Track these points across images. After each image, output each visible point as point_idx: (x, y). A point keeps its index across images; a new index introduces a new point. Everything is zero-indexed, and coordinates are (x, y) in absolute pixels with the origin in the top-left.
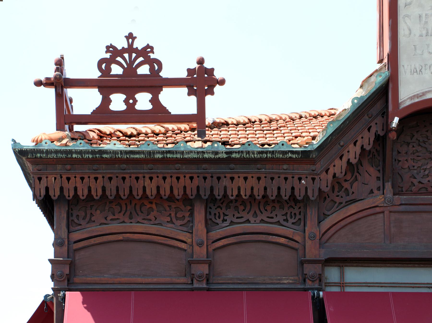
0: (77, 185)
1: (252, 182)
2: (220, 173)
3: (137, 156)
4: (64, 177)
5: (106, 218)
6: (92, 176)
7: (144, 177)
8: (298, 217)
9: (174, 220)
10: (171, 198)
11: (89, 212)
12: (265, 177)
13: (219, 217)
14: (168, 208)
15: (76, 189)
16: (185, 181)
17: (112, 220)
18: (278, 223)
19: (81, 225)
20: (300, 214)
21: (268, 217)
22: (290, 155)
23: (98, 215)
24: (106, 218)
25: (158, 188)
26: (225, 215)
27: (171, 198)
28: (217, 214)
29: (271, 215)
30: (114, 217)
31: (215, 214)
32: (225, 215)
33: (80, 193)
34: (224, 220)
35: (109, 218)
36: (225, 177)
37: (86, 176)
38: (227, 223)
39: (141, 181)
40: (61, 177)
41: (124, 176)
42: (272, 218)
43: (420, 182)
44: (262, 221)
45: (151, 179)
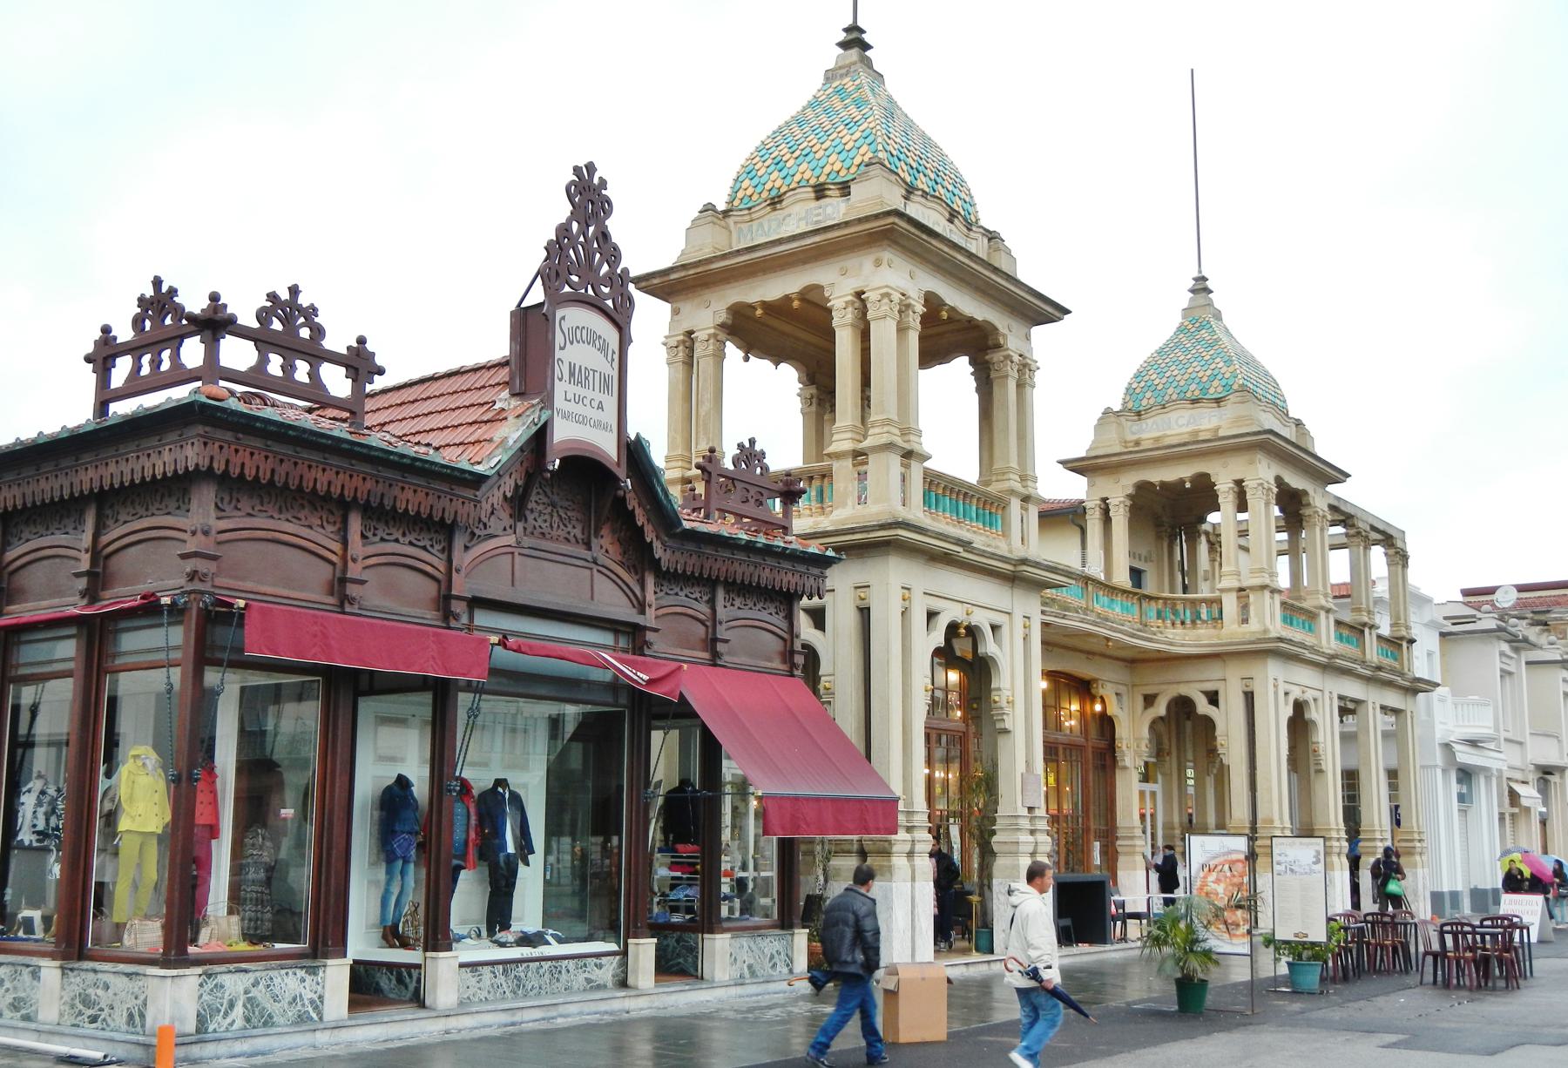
1: (421, 495)
2: (284, 454)
3: (324, 441)
5: (253, 509)
14: (320, 509)
15: (243, 465)
16: (357, 481)
17: (260, 511)
18: (424, 548)
19: (224, 511)
22: (467, 475)
23: (245, 505)
24: (253, 509)
25: (329, 483)
32: (376, 529)
33: (247, 472)
34: (375, 535)
35: (256, 509)
38: (377, 539)
39: (313, 471)
44: (411, 543)
45: (324, 470)
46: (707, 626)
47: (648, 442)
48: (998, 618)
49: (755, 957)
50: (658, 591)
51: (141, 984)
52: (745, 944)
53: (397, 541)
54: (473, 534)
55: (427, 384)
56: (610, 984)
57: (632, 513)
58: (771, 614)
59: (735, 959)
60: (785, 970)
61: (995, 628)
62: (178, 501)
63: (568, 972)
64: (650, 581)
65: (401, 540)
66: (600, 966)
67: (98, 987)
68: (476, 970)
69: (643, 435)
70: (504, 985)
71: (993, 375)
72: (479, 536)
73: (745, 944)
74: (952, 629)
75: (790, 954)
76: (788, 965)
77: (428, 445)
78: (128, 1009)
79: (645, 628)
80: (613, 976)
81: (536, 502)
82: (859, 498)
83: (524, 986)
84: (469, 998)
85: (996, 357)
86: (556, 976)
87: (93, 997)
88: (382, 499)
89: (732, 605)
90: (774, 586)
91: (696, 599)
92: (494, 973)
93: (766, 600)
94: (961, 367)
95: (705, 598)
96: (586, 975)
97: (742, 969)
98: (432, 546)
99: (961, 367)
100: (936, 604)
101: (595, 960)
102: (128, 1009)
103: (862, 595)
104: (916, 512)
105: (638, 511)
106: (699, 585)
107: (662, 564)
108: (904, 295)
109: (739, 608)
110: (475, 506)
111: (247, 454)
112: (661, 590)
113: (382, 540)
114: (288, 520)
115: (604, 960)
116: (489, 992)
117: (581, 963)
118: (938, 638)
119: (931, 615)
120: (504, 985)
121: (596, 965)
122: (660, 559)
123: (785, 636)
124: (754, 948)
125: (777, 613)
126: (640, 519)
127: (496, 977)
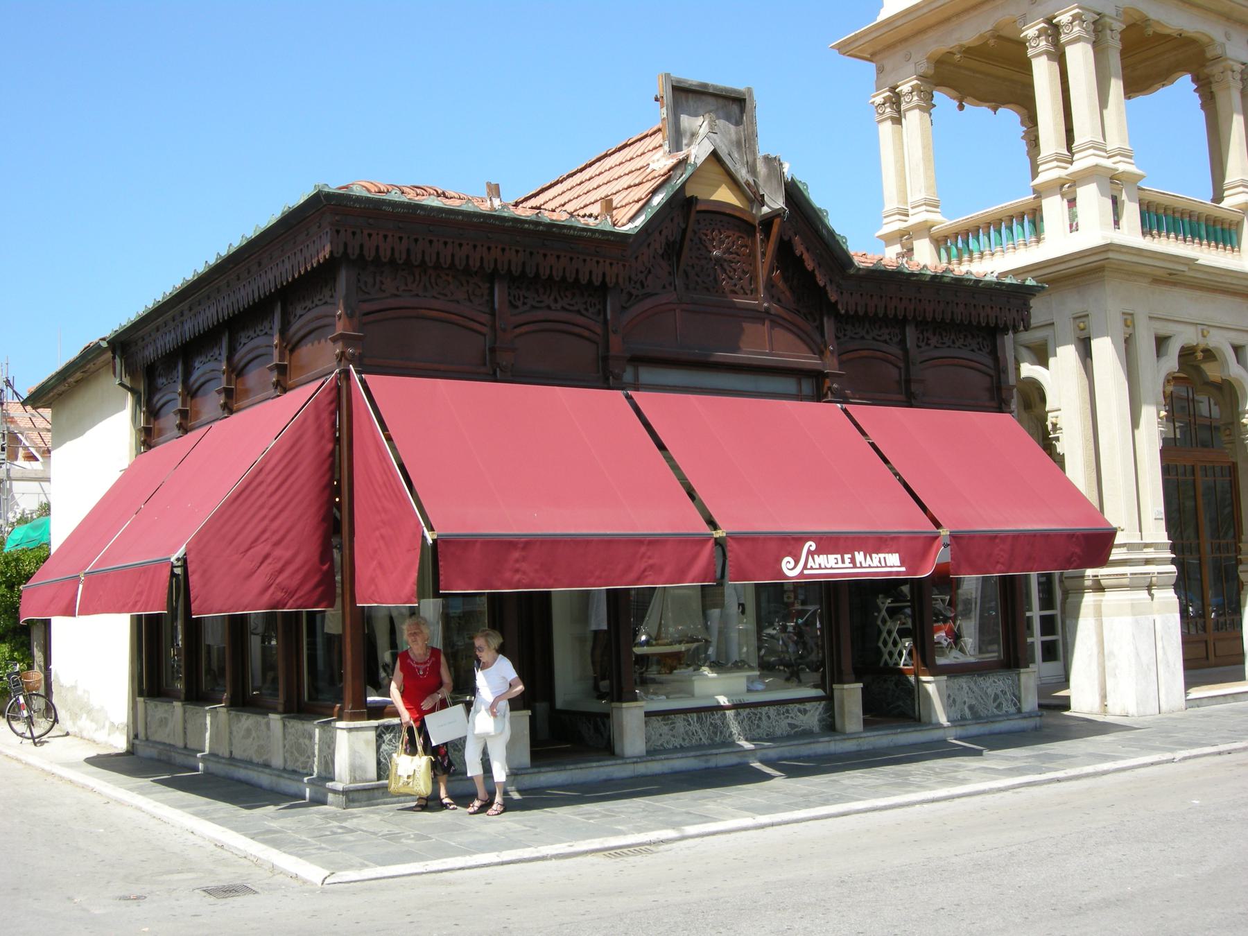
0: (484, 255)
4: (366, 232)
6: (366, 232)
7: (453, 242)
8: (598, 307)
9: (472, 297)
10: (377, 261)
11: (378, 278)
12: (565, 256)
13: (519, 299)
20: (599, 303)
21: (569, 304)
26: (845, 330)
27: (377, 261)
28: (517, 297)
29: (571, 302)
30: (406, 288)
31: (514, 297)
36: (538, 253)
37: (390, 235)
40: (362, 232)
41: (447, 240)
42: (573, 305)
43: (703, 282)
46: (900, 368)
47: (804, 184)
48: (1240, 339)
49: (976, 698)
50: (840, 335)
51: (330, 735)
52: (964, 686)
53: (549, 308)
54: (630, 295)
55: (602, 161)
56: (816, 729)
57: (800, 260)
58: (973, 350)
59: (954, 701)
60: (1013, 710)
61: (1237, 349)
62: (331, 290)
63: (769, 717)
64: (829, 325)
65: (553, 306)
66: (805, 712)
67: (305, 738)
68: (668, 719)
69: (798, 178)
70: (700, 731)
71: (1215, 88)
72: (637, 296)
73: (964, 686)
74: (1187, 354)
75: (1017, 693)
76: (1015, 705)
77: (590, 216)
78: (325, 757)
79: (827, 375)
80: (820, 721)
81: (697, 258)
82: (1071, 226)
83: (721, 733)
84: (662, 745)
85: (1216, 70)
86: (756, 722)
87: (303, 746)
88: (537, 269)
89: (928, 344)
90: (970, 321)
91: (885, 342)
92: (688, 721)
93: (966, 336)
94: (1184, 84)
95: (896, 340)
96: (789, 721)
97: (962, 710)
98: (586, 310)
99: (1184, 84)
100: (1164, 329)
101: (798, 706)
102: (325, 757)
103: (1082, 325)
104: (1130, 234)
105: (806, 256)
106: (887, 327)
107: (840, 307)
108: (1099, 14)
109: (936, 347)
110: (624, 266)
111: (485, 249)
112: (845, 335)
113: (533, 307)
114: (434, 297)
115: (808, 706)
116: (684, 739)
117: (782, 709)
118: (1171, 363)
119: (1161, 342)
120: (700, 731)
121: (800, 711)
122: (836, 302)
123: (992, 372)
124: (975, 689)
125: (980, 349)
126: (810, 265)
127: (690, 724)
